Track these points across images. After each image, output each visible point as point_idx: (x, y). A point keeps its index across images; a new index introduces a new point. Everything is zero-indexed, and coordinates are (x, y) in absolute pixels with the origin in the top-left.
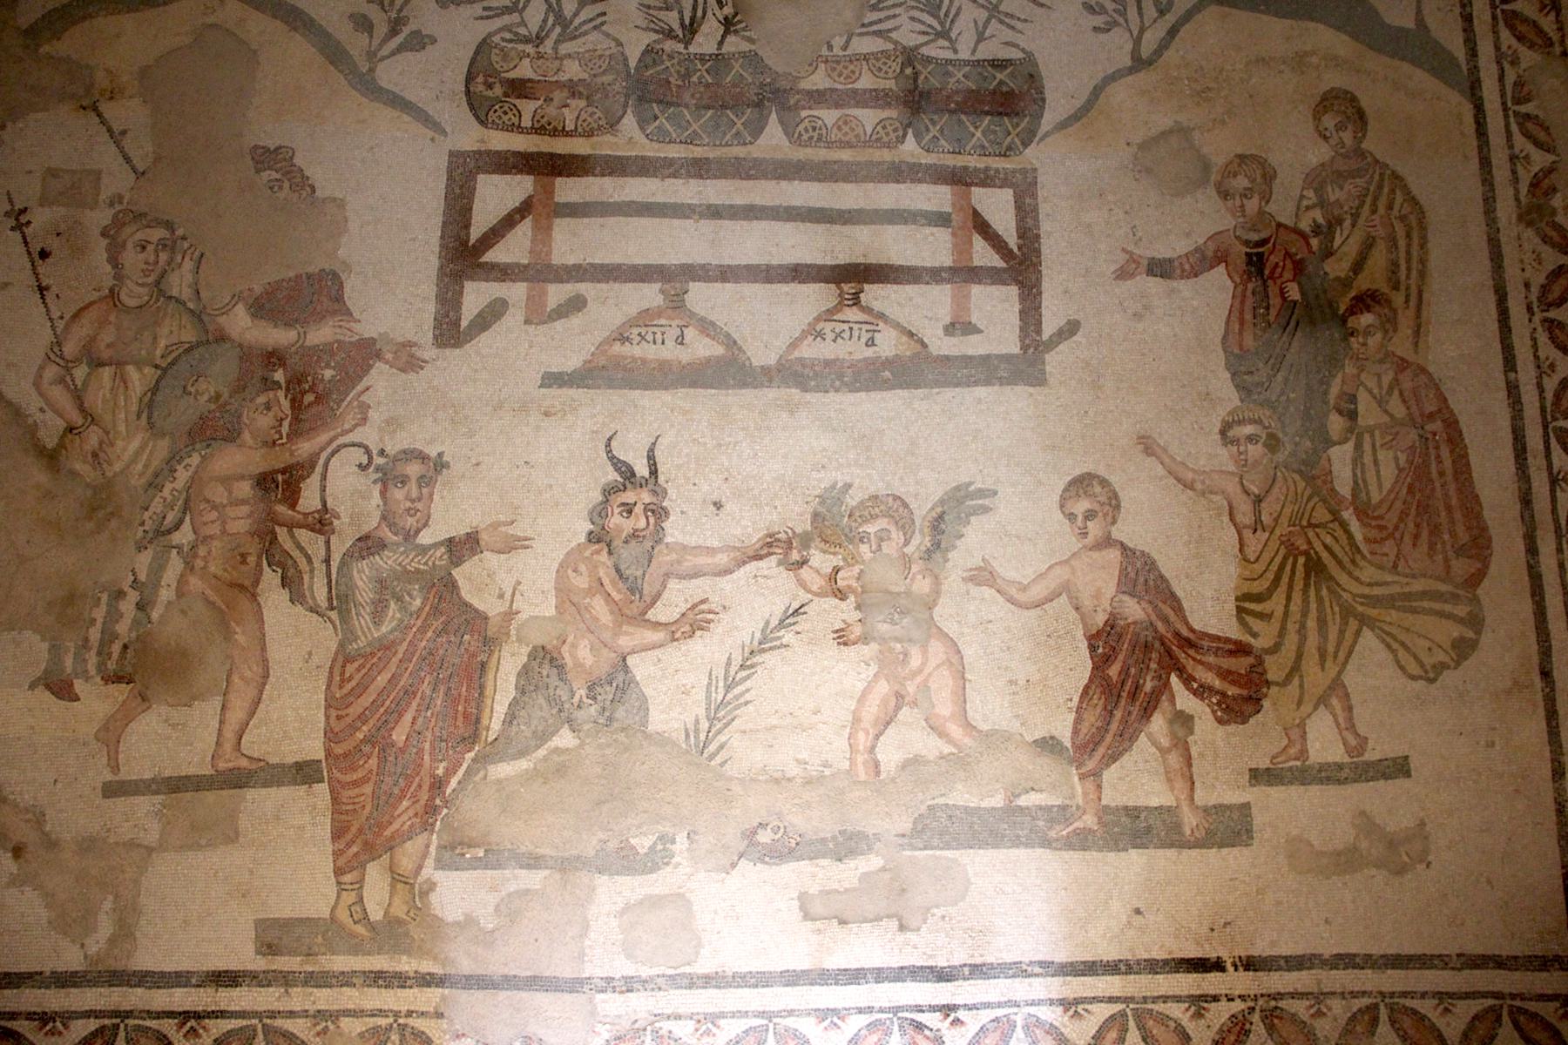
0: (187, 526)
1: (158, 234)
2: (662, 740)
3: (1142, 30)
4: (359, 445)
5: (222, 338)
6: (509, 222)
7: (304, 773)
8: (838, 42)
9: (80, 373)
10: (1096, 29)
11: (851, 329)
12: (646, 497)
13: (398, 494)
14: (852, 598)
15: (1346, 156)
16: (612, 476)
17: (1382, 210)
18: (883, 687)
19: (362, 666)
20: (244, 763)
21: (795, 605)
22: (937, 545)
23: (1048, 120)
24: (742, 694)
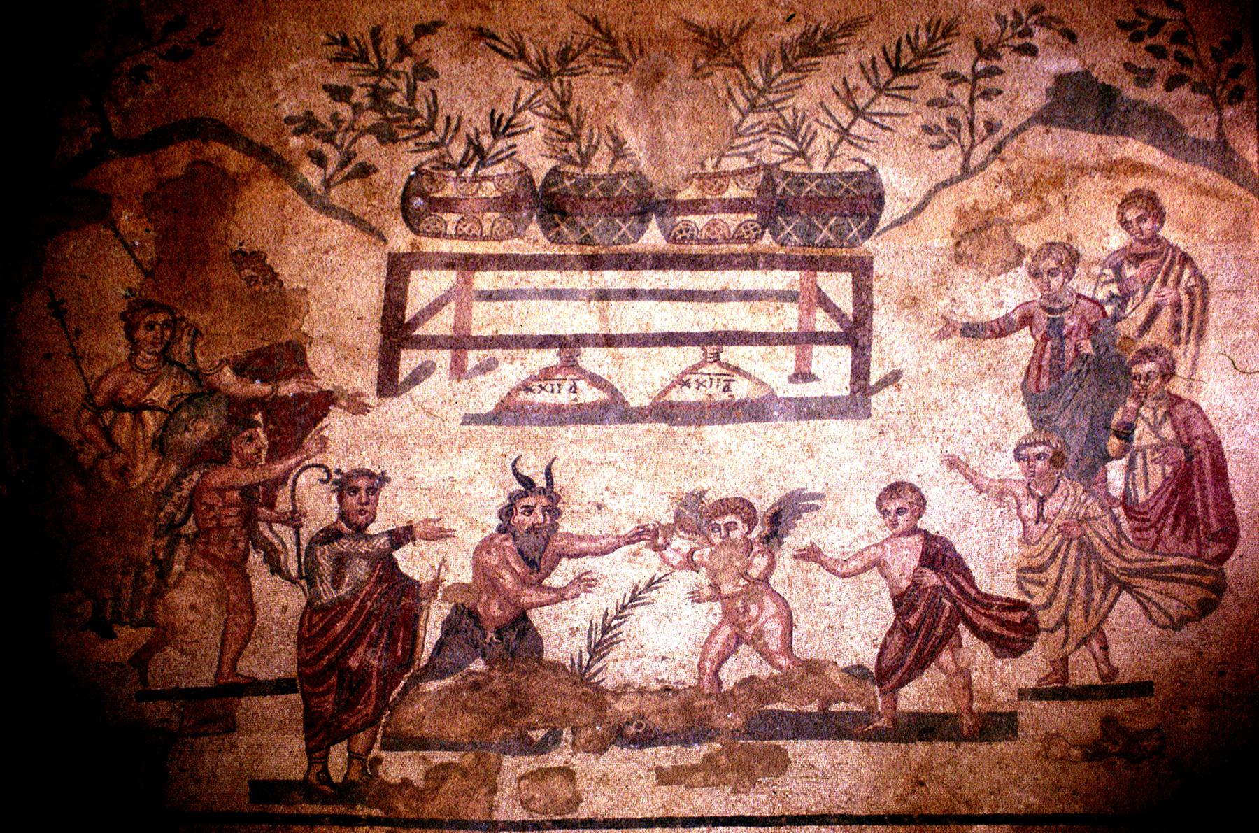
0: (191, 522)
1: (161, 318)
2: (555, 667)
3: (972, 147)
4: (320, 466)
5: (213, 390)
6: (435, 307)
7: (281, 687)
8: (709, 164)
9: (108, 416)
10: (932, 147)
11: (711, 379)
12: (544, 502)
13: (352, 500)
14: (704, 569)
15: (1144, 242)
16: (516, 486)
17: (1170, 284)
18: (727, 630)
19: (324, 617)
20: (239, 680)
21: (660, 574)
22: (774, 533)
23: (886, 218)
24: (615, 636)
